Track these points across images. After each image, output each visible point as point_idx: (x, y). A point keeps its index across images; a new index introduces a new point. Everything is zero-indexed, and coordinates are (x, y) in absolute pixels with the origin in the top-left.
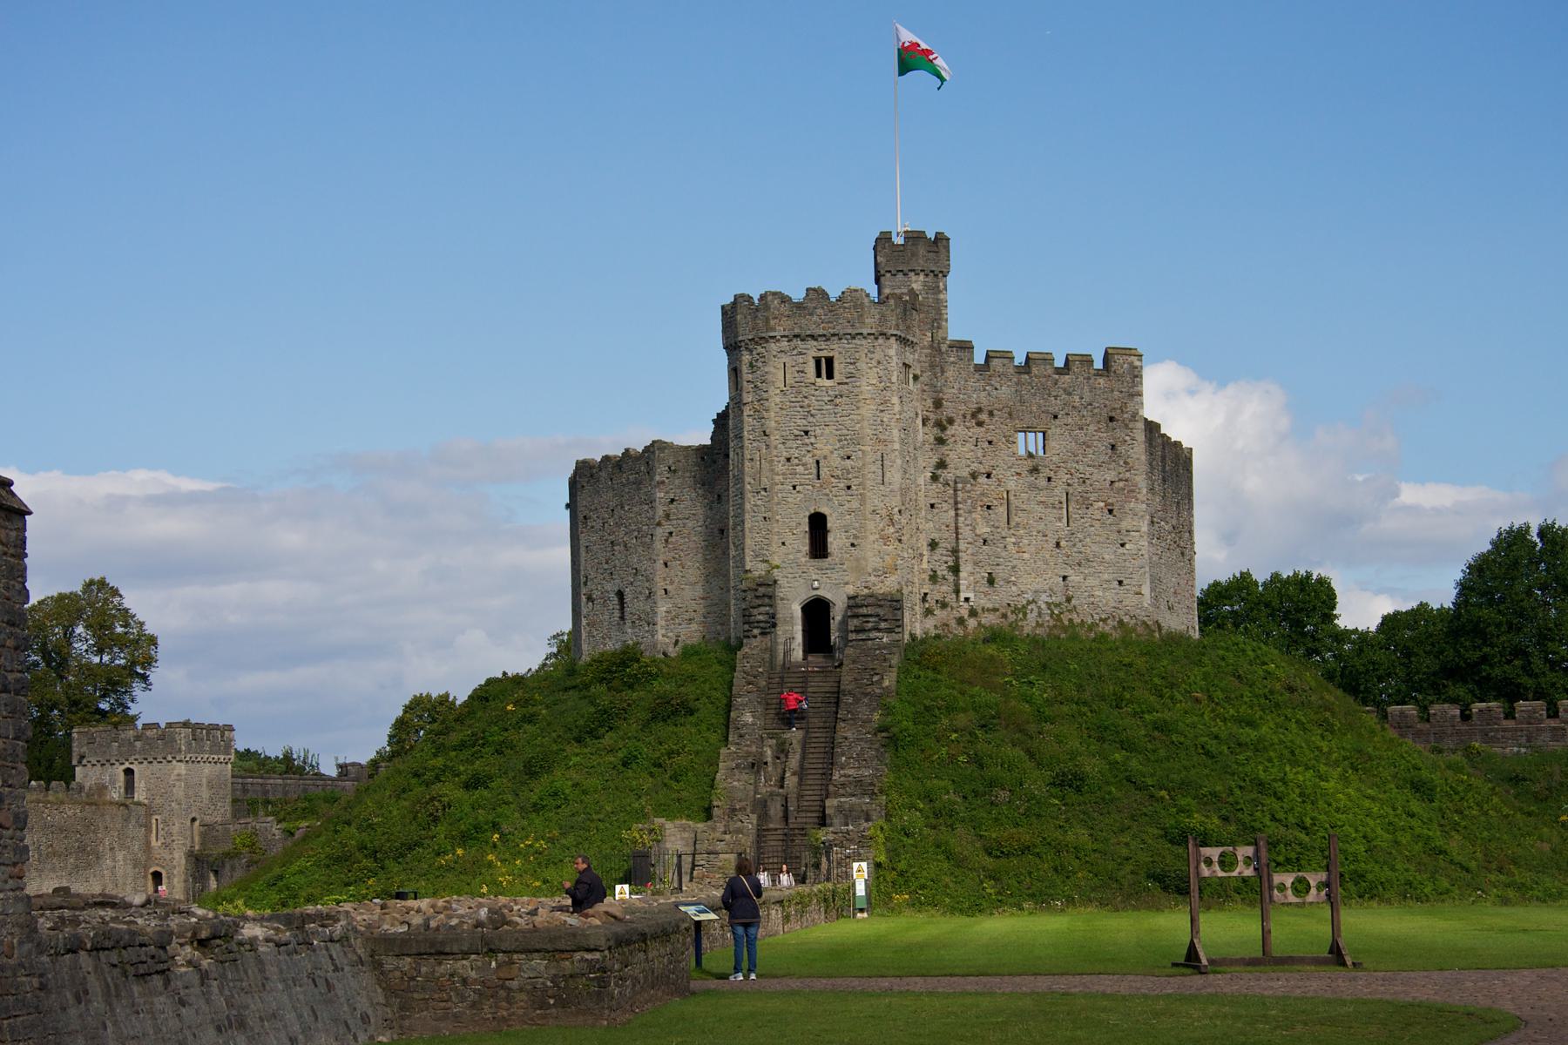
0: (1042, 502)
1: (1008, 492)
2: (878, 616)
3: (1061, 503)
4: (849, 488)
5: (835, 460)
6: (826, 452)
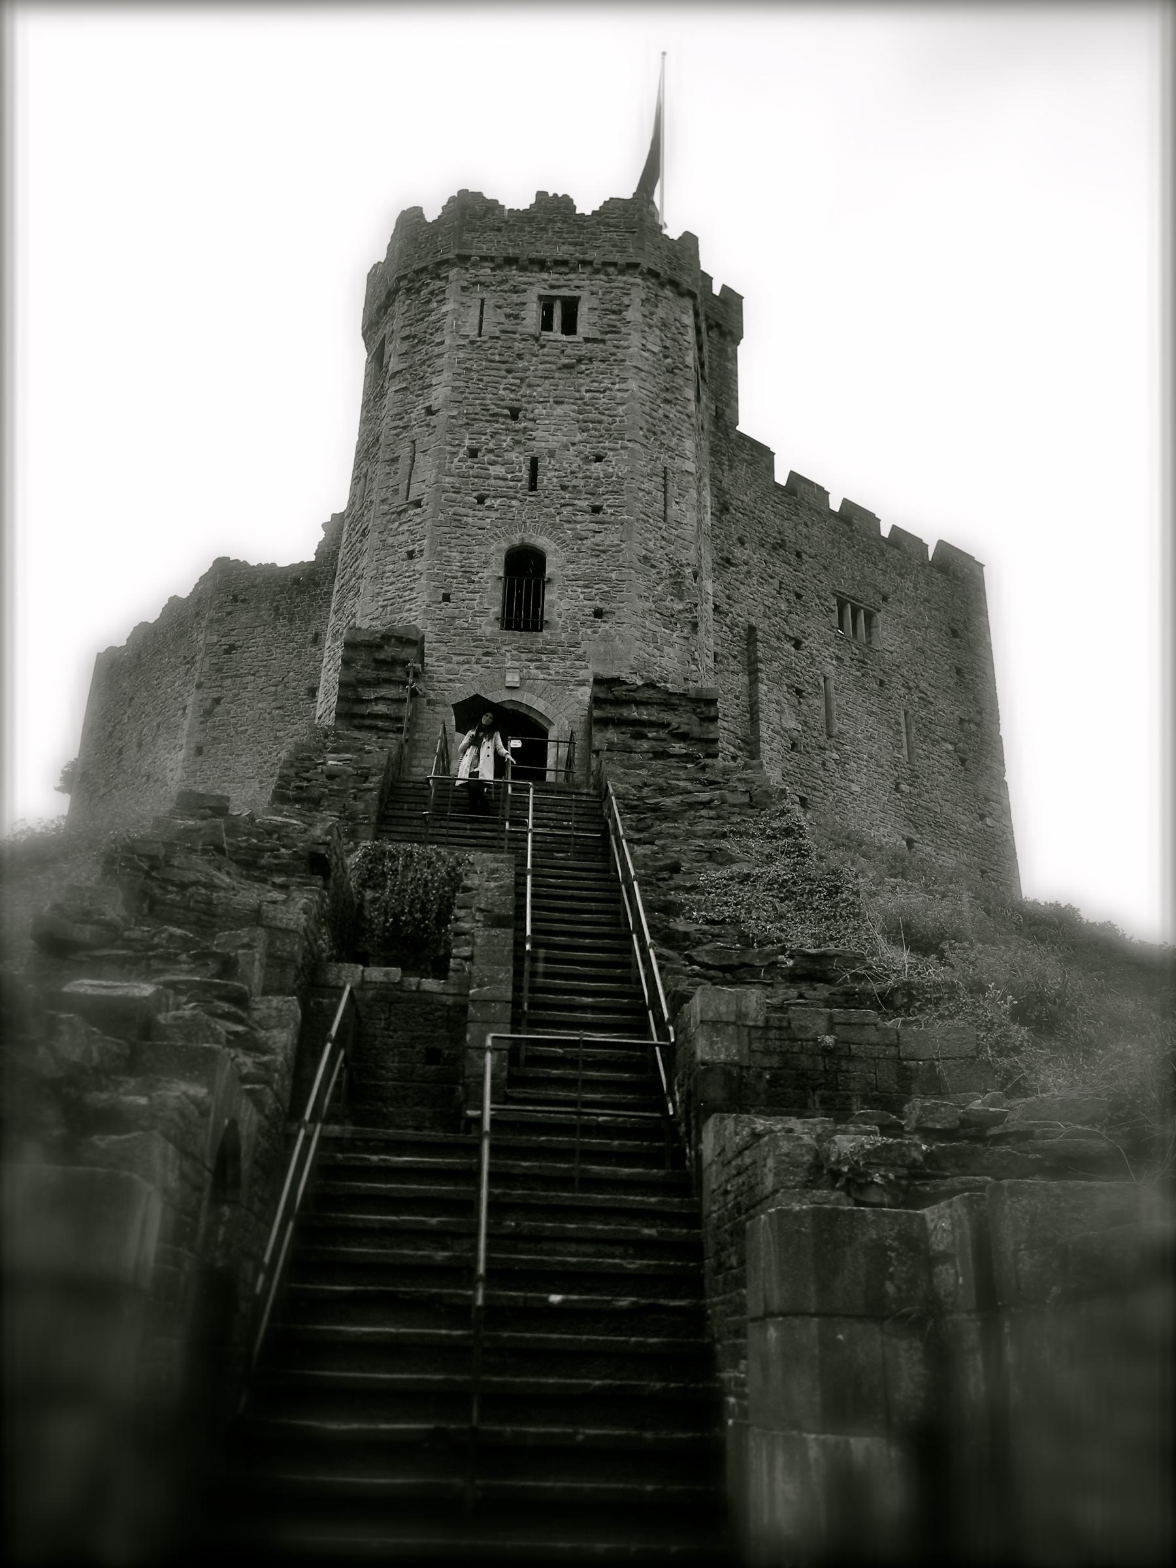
0: (873, 712)
1: (826, 679)
2: (669, 725)
3: (899, 724)
4: (596, 510)
5: (571, 460)
6: (554, 445)
